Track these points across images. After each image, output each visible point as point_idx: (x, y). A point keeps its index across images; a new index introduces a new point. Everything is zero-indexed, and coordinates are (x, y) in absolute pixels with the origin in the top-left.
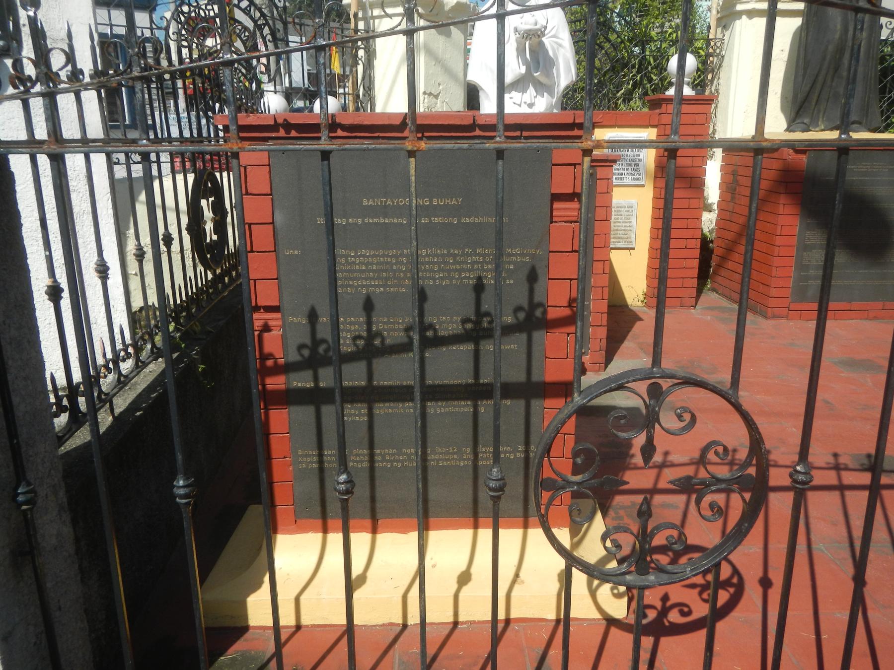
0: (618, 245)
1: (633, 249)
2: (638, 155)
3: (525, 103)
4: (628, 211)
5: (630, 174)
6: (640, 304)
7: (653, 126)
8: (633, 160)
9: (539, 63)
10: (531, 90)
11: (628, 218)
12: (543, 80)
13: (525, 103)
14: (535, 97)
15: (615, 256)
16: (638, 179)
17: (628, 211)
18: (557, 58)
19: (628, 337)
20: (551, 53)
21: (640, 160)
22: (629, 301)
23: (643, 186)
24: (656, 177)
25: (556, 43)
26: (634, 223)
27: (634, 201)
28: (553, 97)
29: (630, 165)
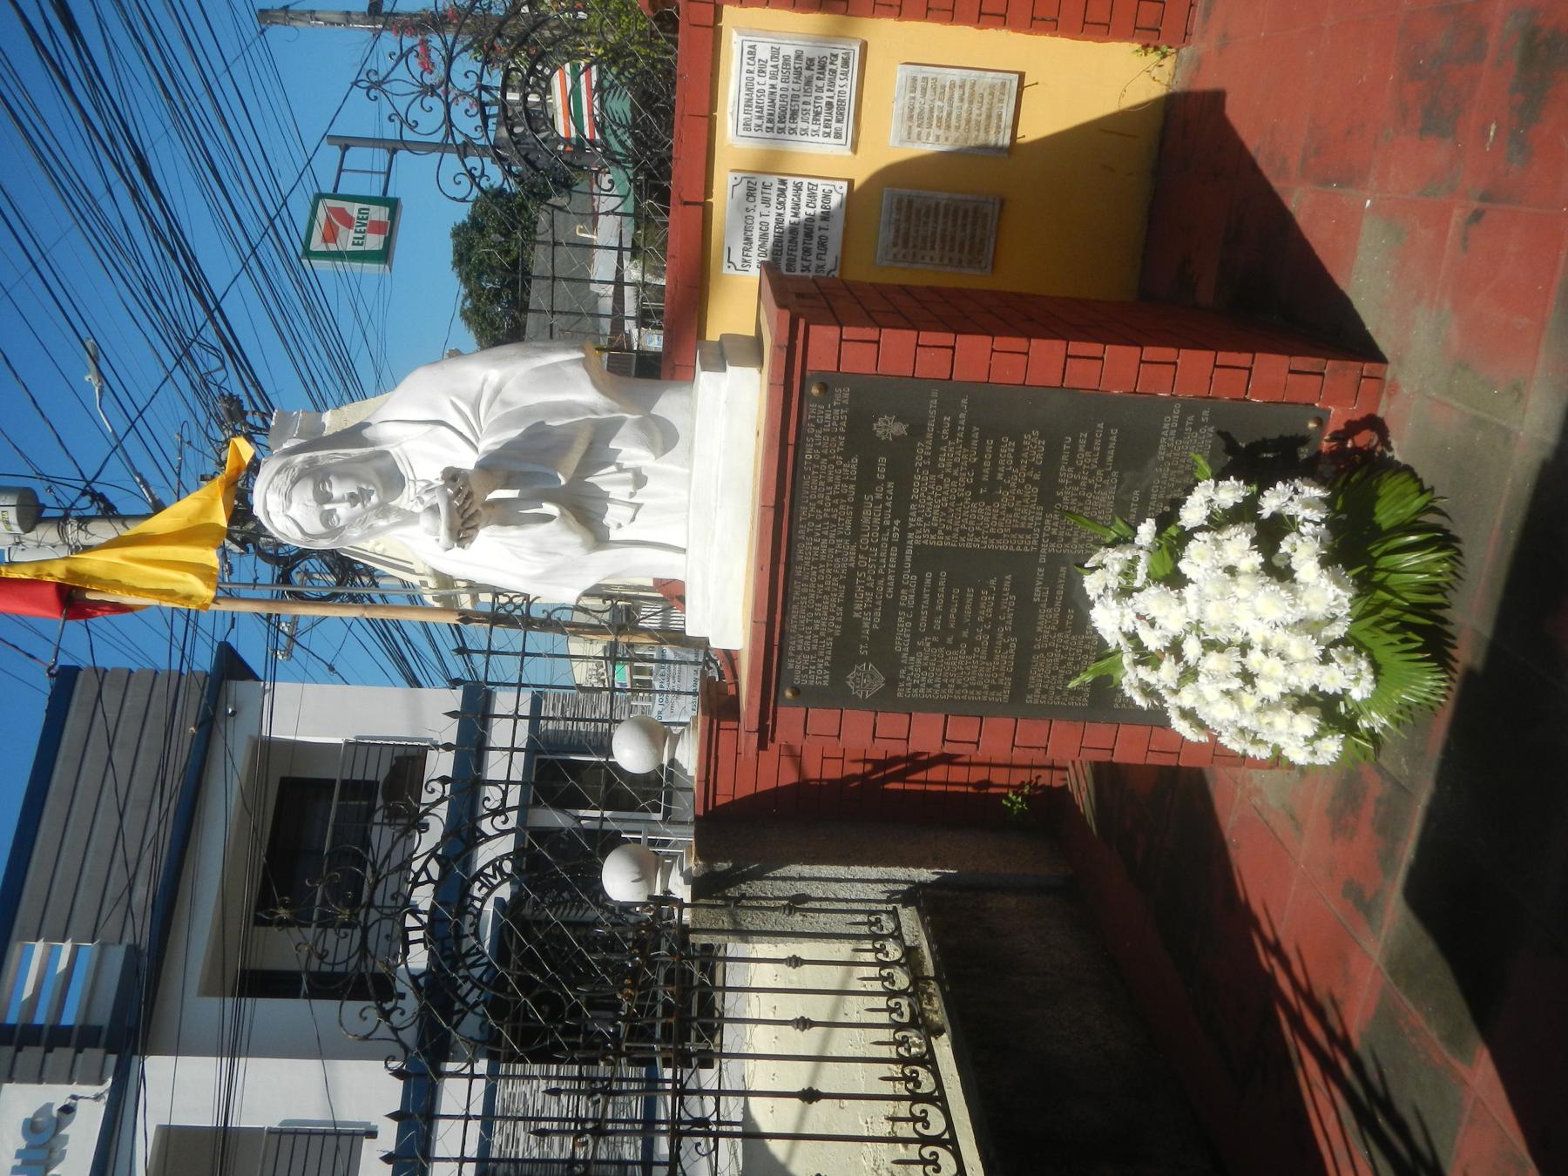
0: (1007, 118)
1: (1022, 76)
2: (786, 59)
3: (632, 495)
4: (924, 90)
5: (832, 83)
6: (1169, 63)
7: (718, 16)
8: (798, 72)
9: (536, 473)
10: (603, 479)
11: (940, 90)
12: (574, 459)
13: (632, 495)
14: (621, 469)
15: (1033, 129)
16: (846, 63)
17: (924, 90)
18: (528, 411)
19: (1277, 185)
20: (513, 434)
21: (798, 57)
22: (1157, 91)
23: (864, 47)
24: (846, 13)
25: (490, 403)
26: (956, 75)
27: (901, 74)
28: (619, 423)
29: (809, 82)
